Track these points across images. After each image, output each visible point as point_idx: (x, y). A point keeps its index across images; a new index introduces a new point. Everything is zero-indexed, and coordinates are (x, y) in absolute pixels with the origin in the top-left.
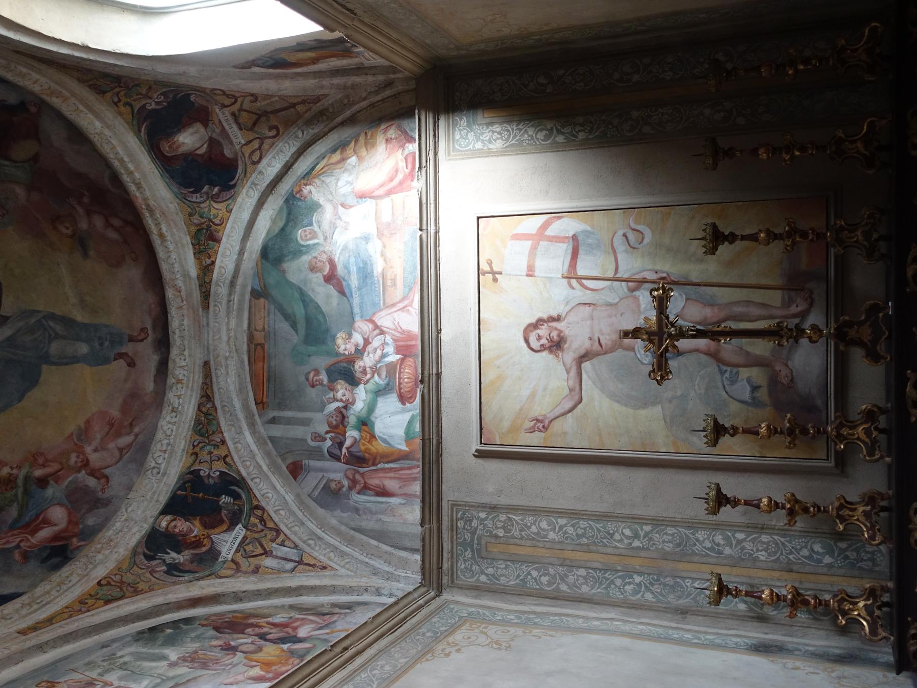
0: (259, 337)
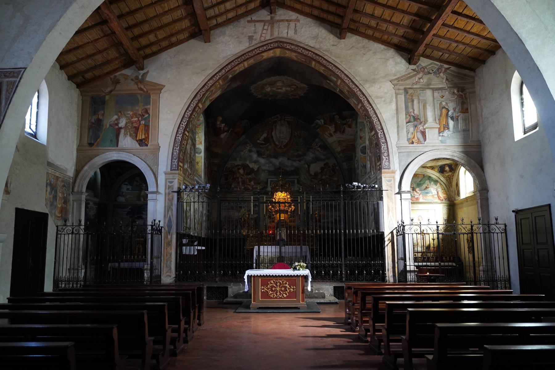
0: (418, 176)
